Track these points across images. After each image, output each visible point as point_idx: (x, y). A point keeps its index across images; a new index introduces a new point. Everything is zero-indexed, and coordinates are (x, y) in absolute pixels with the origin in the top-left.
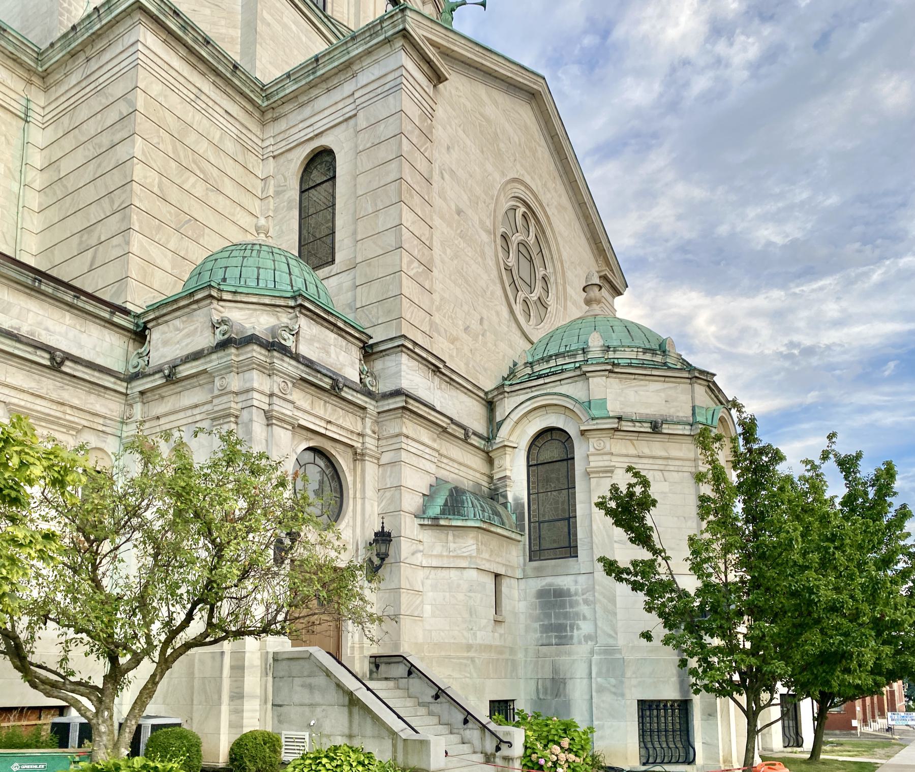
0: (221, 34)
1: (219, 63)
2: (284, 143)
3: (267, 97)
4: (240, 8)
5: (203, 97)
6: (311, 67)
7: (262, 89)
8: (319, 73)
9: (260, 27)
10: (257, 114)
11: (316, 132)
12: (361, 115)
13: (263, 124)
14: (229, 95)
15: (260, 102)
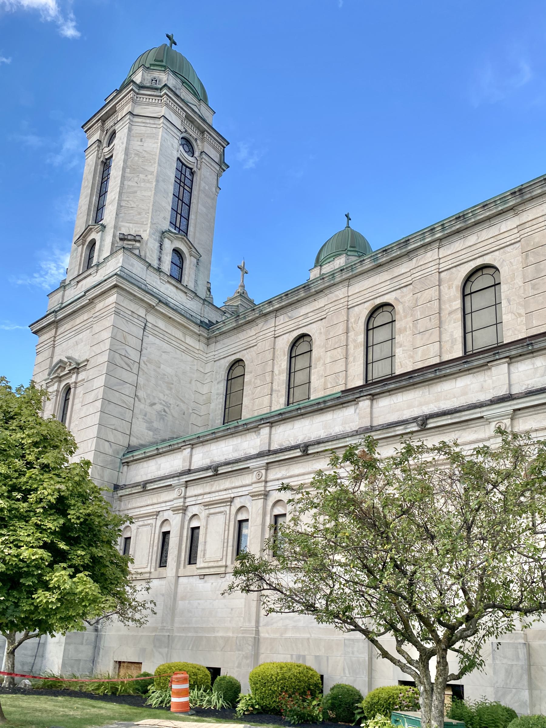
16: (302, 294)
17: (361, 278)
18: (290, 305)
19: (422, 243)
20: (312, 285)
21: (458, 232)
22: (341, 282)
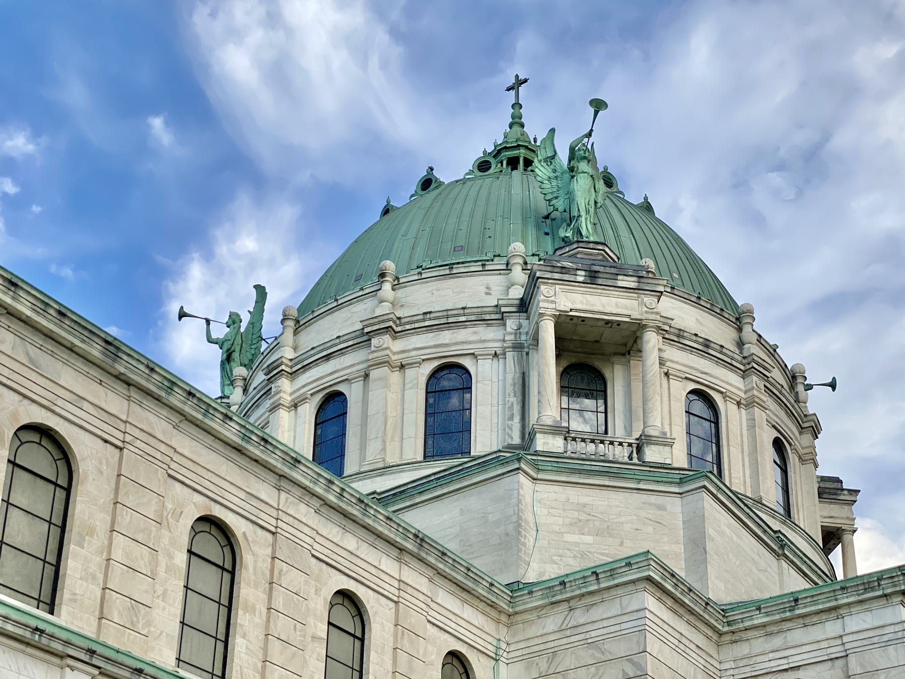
2: (748, 669)
3: (729, 624)
5: (684, 640)
6: (787, 605)
7: (724, 616)
8: (798, 612)
9: (709, 546)
10: (715, 637)
11: (791, 665)
12: (852, 659)
13: (718, 645)
15: (720, 627)
17: (202, 435)
19: (311, 485)
20: (125, 357)
21: (345, 515)
22: (172, 408)
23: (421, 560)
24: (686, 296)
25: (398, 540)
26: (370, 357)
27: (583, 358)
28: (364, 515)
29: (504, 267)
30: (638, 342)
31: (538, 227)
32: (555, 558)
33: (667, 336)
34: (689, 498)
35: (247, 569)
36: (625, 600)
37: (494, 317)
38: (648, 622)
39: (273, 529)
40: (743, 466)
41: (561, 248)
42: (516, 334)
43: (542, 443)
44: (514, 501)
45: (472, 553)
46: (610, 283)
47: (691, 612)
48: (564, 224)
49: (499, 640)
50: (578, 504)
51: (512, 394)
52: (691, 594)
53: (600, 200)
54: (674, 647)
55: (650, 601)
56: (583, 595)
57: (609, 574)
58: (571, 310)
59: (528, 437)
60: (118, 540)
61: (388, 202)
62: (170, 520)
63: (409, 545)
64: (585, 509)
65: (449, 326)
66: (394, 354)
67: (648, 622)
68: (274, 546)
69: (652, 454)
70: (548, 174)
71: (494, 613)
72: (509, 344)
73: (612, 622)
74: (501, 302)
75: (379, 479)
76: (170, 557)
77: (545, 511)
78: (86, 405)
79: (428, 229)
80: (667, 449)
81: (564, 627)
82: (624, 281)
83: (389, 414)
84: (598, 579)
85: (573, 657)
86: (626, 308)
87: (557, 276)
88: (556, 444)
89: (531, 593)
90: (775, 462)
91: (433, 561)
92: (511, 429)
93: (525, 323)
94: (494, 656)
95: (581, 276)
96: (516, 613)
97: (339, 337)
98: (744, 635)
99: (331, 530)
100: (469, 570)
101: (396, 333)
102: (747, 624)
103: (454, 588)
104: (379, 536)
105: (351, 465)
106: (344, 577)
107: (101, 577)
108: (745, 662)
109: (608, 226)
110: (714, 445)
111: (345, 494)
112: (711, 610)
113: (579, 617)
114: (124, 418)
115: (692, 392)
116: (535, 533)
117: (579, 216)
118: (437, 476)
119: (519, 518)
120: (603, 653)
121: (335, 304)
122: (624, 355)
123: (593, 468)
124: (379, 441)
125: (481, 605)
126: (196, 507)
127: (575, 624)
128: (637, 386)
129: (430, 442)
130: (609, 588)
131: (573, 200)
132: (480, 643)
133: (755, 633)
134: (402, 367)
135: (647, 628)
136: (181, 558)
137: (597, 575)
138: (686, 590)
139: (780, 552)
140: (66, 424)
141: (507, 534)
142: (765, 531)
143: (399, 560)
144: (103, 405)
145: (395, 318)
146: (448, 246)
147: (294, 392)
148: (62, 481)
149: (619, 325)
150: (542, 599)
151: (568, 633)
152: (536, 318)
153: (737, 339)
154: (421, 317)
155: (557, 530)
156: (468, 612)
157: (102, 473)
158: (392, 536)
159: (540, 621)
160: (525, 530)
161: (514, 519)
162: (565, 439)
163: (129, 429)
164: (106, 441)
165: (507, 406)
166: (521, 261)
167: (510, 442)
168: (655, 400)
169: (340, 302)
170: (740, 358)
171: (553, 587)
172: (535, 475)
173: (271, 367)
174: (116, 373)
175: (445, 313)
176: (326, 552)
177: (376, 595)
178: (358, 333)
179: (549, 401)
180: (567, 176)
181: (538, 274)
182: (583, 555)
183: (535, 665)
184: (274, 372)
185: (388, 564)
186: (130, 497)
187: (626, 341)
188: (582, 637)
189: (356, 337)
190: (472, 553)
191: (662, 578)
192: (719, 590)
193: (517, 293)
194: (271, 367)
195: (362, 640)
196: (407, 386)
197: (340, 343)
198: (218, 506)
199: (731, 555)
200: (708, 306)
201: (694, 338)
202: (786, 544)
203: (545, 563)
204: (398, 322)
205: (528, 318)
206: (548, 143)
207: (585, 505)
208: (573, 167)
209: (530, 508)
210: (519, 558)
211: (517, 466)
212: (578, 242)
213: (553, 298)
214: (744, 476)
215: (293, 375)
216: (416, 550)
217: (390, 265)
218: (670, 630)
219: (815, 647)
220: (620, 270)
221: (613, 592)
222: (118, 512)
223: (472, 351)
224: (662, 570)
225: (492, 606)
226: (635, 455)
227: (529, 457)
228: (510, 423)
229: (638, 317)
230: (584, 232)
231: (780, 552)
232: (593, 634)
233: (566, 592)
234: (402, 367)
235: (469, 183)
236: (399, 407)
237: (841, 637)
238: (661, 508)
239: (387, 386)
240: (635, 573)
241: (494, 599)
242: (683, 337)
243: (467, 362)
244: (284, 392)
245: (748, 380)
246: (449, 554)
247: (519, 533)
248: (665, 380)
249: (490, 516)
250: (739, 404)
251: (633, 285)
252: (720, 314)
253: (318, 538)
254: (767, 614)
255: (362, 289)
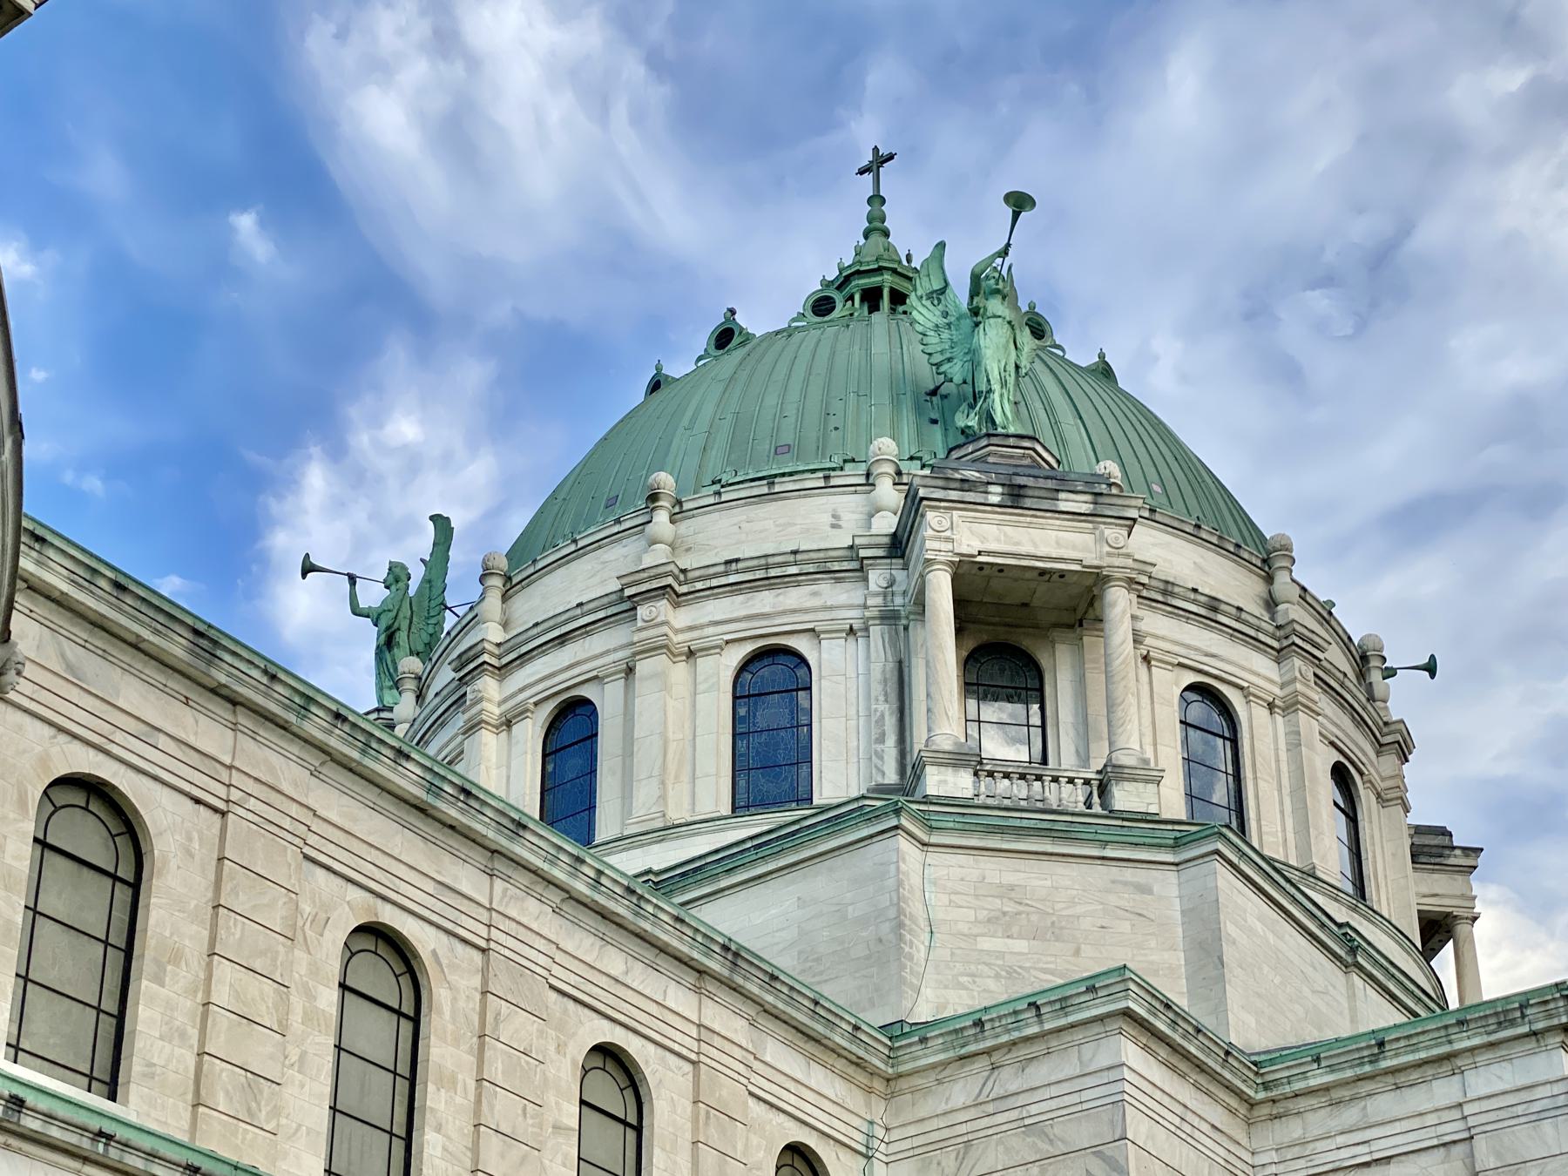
0: (1152, 963)
1: (1208, 1056)
3: (1266, 1086)
4: (1178, 915)
5: (1189, 1117)
7: (1257, 1074)
9: (1229, 953)
10: (1243, 1110)
14: (1208, 1094)
15: (1251, 1093)
16: (177, 647)
17: (358, 786)
18: (98, 624)
19: (546, 867)
20: (227, 657)
21: (604, 915)
22: (308, 741)
23: (735, 989)
24: (1176, 524)
25: (695, 955)
26: (636, 639)
27: (1002, 635)
28: (637, 914)
29: (862, 480)
30: (1096, 604)
31: (919, 410)
32: (964, 979)
33: (1145, 593)
34: (1192, 871)
35: (440, 1013)
36: (1087, 1050)
37: (846, 566)
38: (1128, 1088)
39: (483, 944)
40: (1282, 812)
41: (959, 447)
42: (885, 596)
43: (937, 782)
44: (891, 882)
45: (821, 973)
46: (1046, 505)
47: (1201, 1067)
48: (964, 406)
49: (871, 1123)
50: (1001, 885)
51: (882, 698)
52: (1200, 1037)
53: (1025, 363)
54: (1173, 1129)
55: (1131, 1051)
56: (1014, 1043)
57: (1058, 1006)
58: (980, 553)
59: (911, 771)
60: (223, 970)
61: (659, 368)
62: (309, 933)
63: (715, 965)
64: (1013, 895)
65: (769, 583)
66: (677, 632)
67: (1128, 1088)
68: (485, 972)
69: (1125, 797)
70: (934, 319)
71: (862, 1077)
72: (874, 612)
73: (1066, 1088)
74: (858, 541)
75: (656, 847)
76: (310, 996)
77: (945, 899)
78: (163, 742)
79: (729, 417)
80: (1152, 787)
81: (981, 1099)
82: (1068, 502)
83: (670, 735)
84: (1039, 1015)
85: (1001, 1148)
86: (1074, 548)
87: (954, 495)
88: (960, 783)
89: (923, 1040)
90: (1336, 804)
91: (755, 990)
92: (882, 758)
93: (900, 575)
94: (863, 1150)
95: (995, 495)
96: (900, 1076)
97: (580, 605)
98: (1291, 1105)
99: (581, 942)
100: (817, 1003)
101: (678, 596)
102: (1298, 1086)
103: (791, 1035)
104: (663, 949)
105: (606, 825)
106: (605, 1022)
107: (194, 1033)
108: (1296, 1151)
109: (1038, 405)
110: (1231, 778)
111: (604, 880)
112: (1235, 1064)
113: (1009, 1080)
114: (228, 761)
115: (1191, 688)
116: (928, 936)
117: (990, 391)
118: (756, 842)
119: (900, 912)
120: (1051, 1141)
121: (573, 548)
122: (1071, 626)
123: (1025, 823)
124: (655, 782)
125: (840, 1064)
126: (352, 909)
127: (1002, 1093)
128: (1095, 680)
129: (742, 783)
130: (1059, 1030)
131: (979, 363)
132: (840, 1130)
133: (1313, 1101)
134: (691, 654)
135: (1126, 1097)
136: (329, 997)
137: (1038, 1008)
138: (1190, 1030)
139: (1349, 960)
140: (131, 774)
141: (880, 940)
142: (1322, 926)
143: (697, 990)
144: (192, 740)
145: (676, 571)
146: (765, 446)
147: (505, 701)
148: (126, 872)
149: (1062, 576)
150: (945, 1050)
151: (990, 1108)
152: (920, 568)
153: (1266, 595)
154: (721, 568)
155: (966, 931)
156: (818, 1077)
157: (192, 856)
158: (685, 949)
159: (940, 1088)
160: (910, 932)
161: (892, 913)
162: (976, 774)
163: (236, 778)
164: (198, 801)
165: (874, 719)
166: (890, 469)
167: (880, 781)
168: (1128, 706)
169: (581, 544)
170: (1271, 629)
171: (962, 1029)
172: (925, 838)
173: (464, 658)
174: (213, 685)
175: (763, 561)
176: (573, 979)
177: (660, 1050)
178: (614, 597)
179: (945, 710)
180: (967, 323)
181: (922, 493)
182: (1011, 973)
183: (934, 1166)
184: (470, 666)
185: (680, 998)
186: (240, 896)
187: (1073, 603)
188: (1014, 1115)
189: (611, 605)
190: (821, 973)
191: (1149, 1011)
192: (1248, 1029)
193: (886, 524)
194: (464, 658)
195: (638, 1129)
196: (700, 688)
197: (583, 615)
198: (389, 907)
199: (1266, 969)
200: (1214, 540)
201: (1192, 596)
202: (1359, 946)
203: (946, 987)
204: (682, 577)
205: (905, 567)
206: (934, 267)
207: (1012, 888)
208: (978, 308)
209: (918, 894)
210: (902, 980)
211: (894, 822)
212: (988, 435)
213: (948, 533)
214: (1284, 830)
215: (503, 671)
216: (726, 973)
217: (665, 480)
218: (1166, 1100)
219: (1416, 1123)
220: (1062, 482)
221: (1066, 1037)
222: (221, 922)
223: (810, 626)
224: (1149, 998)
225: (857, 1065)
226: (1096, 799)
227: (914, 807)
228: (879, 747)
229: (1096, 563)
230: (998, 418)
231: (1349, 960)
232: (1034, 1109)
233: (984, 1039)
234: (691, 654)
235: (797, 337)
236: (687, 725)
237: (1460, 1105)
238: (1145, 889)
239: (666, 688)
240: (1104, 1004)
241: (861, 1053)
242: (1172, 594)
243: (801, 645)
244: (489, 700)
245: (1286, 665)
246: (782, 977)
247: (901, 938)
248: (1143, 669)
249: (850, 908)
250: (1271, 706)
251: (1085, 508)
252: (1235, 554)
253: (559, 957)
254: (1332, 1069)
255: (618, 521)
